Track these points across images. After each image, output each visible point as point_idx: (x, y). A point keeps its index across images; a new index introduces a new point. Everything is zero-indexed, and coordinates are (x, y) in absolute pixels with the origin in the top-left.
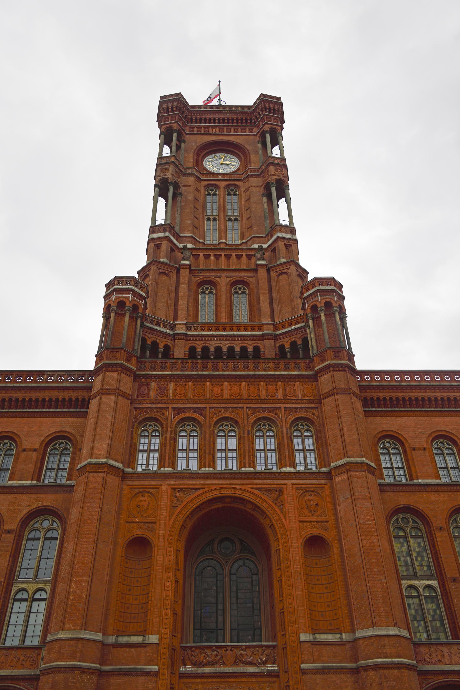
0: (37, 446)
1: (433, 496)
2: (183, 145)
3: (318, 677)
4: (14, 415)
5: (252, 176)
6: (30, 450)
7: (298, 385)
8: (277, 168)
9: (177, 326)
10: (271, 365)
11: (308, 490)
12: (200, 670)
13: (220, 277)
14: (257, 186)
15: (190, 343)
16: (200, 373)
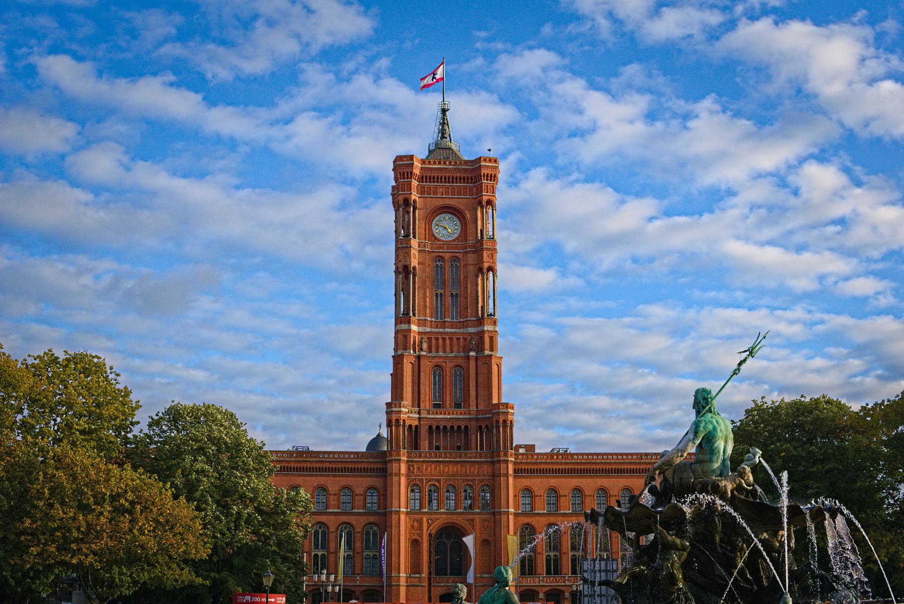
0: (362, 493)
1: (540, 519)
2: (417, 211)
3: (481, 588)
4: (348, 476)
6: (359, 495)
7: (485, 466)
8: (489, 252)
9: (422, 411)
10: (473, 455)
11: (485, 520)
12: (440, 584)
13: (446, 362)
14: (473, 265)
15: (429, 423)
16: (438, 460)
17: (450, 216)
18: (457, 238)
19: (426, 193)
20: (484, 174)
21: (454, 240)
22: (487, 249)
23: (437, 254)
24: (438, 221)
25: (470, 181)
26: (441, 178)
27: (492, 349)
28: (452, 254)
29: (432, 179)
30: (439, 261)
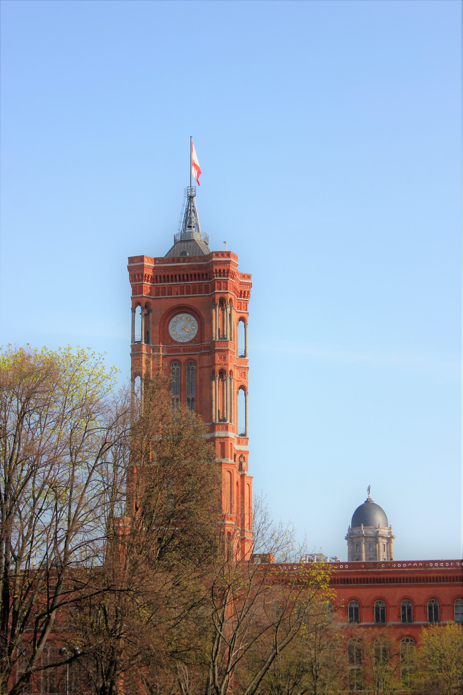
2: (151, 315)
5: (204, 354)
8: (221, 353)
14: (208, 367)
17: (187, 315)
18: (194, 339)
19: (161, 294)
20: (216, 270)
21: (190, 342)
22: (219, 351)
23: (173, 357)
24: (175, 322)
25: (205, 277)
26: (176, 276)
27: (223, 456)
28: (188, 357)
29: (166, 279)
30: (175, 365)
